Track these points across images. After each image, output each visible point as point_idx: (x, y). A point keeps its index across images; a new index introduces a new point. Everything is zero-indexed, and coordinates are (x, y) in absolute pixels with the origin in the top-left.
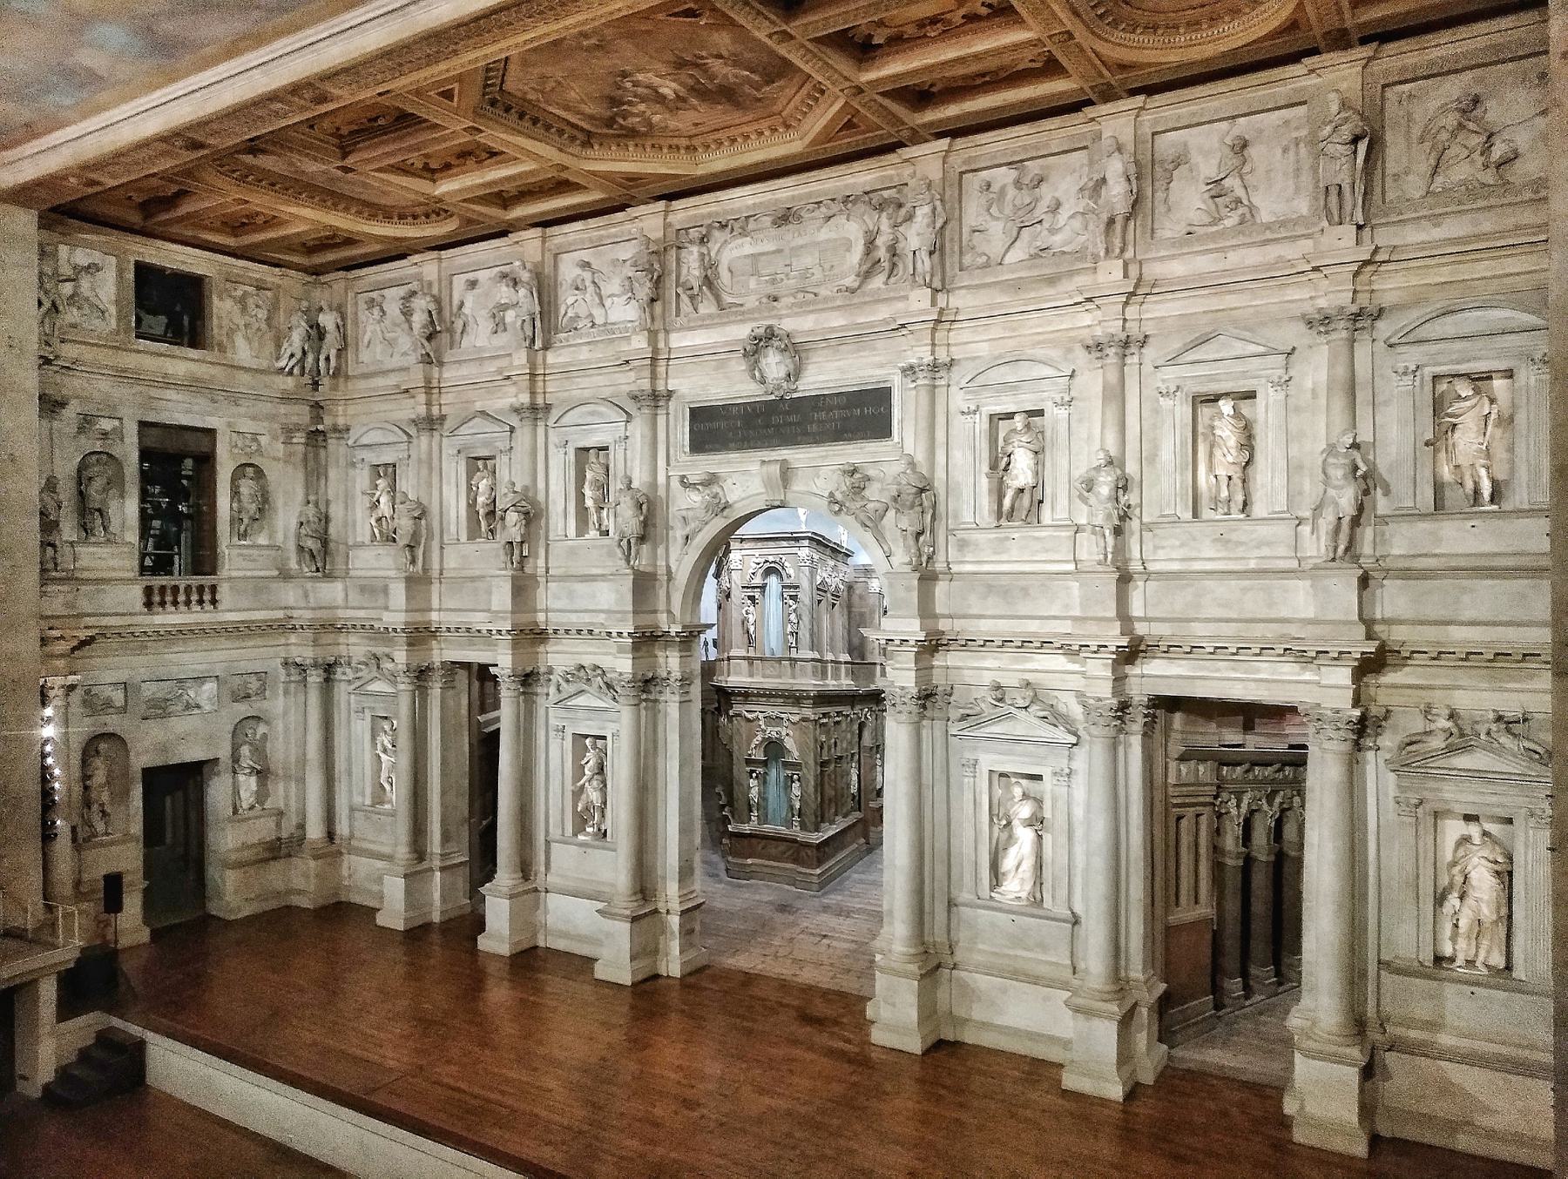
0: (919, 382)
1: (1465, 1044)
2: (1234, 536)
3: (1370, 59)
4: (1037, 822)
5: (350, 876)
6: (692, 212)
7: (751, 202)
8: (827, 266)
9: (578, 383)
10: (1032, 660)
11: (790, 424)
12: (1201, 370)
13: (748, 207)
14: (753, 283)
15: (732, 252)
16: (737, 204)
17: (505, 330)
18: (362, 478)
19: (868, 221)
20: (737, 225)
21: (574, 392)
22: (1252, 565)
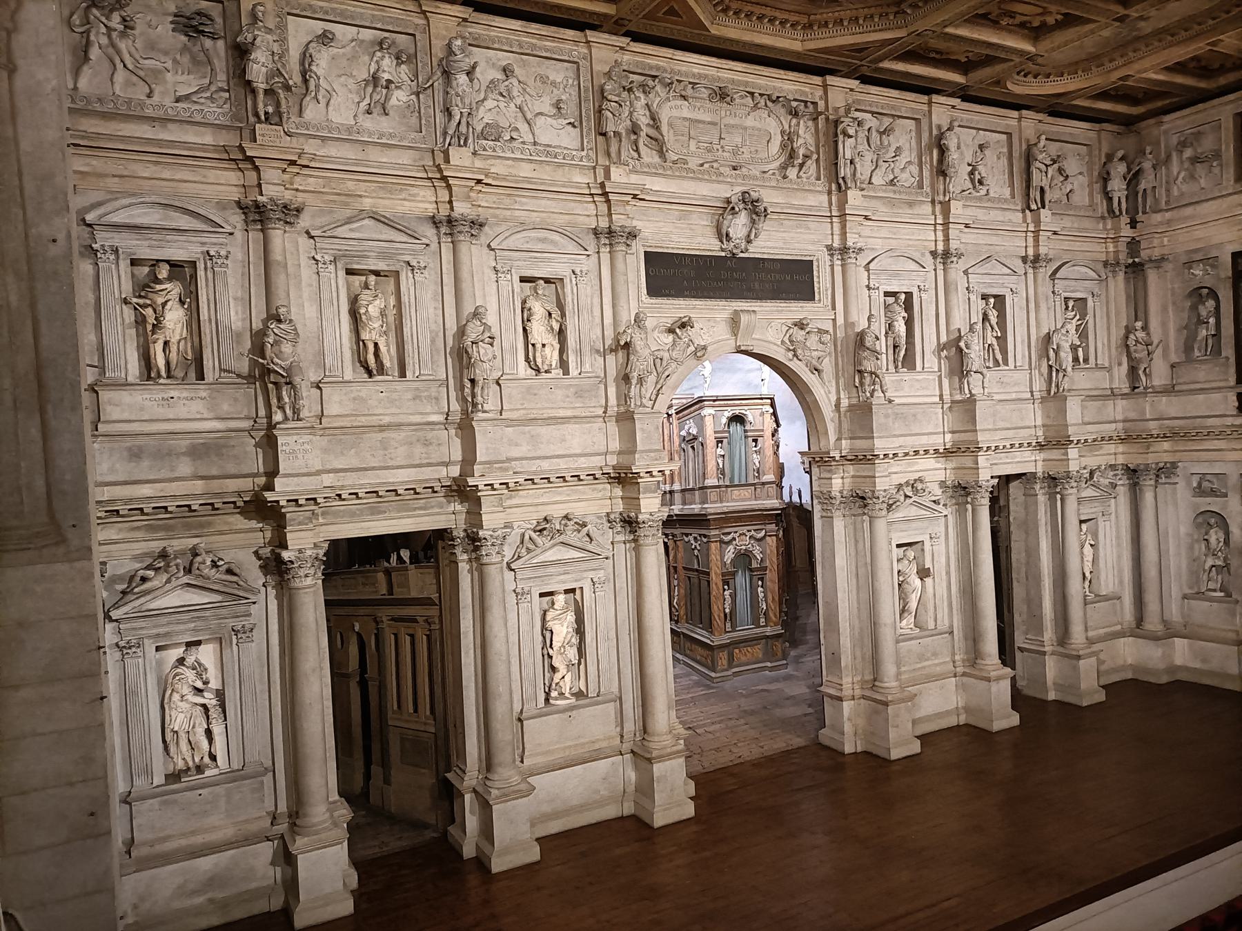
0: (849, 260)
1: (1102, 631)
2: (1005, 380)
3: (1040, 121)
4: (924, 573)
5: (135, 907)
6: (639, 58)
7: (696, 71)
8: (753, 149)
9: (522, 204)
10: (917, 463)
11: (736, 279)
12: (987, 279)
13: (694, 75)
14: (693, 144)
15: (673, 111)
16: (684, 68)
17: (387, 114)
18: (119, 281)
19: (784, 122)
20: (680, 87)
21: (517, 213)
22: (1014, 396)
